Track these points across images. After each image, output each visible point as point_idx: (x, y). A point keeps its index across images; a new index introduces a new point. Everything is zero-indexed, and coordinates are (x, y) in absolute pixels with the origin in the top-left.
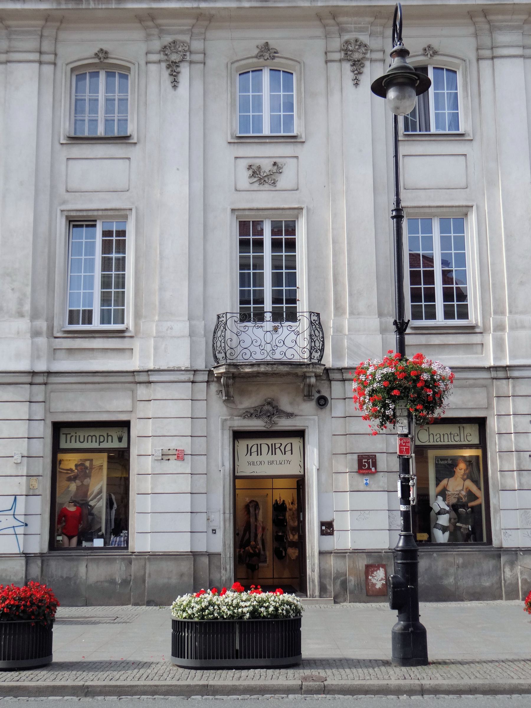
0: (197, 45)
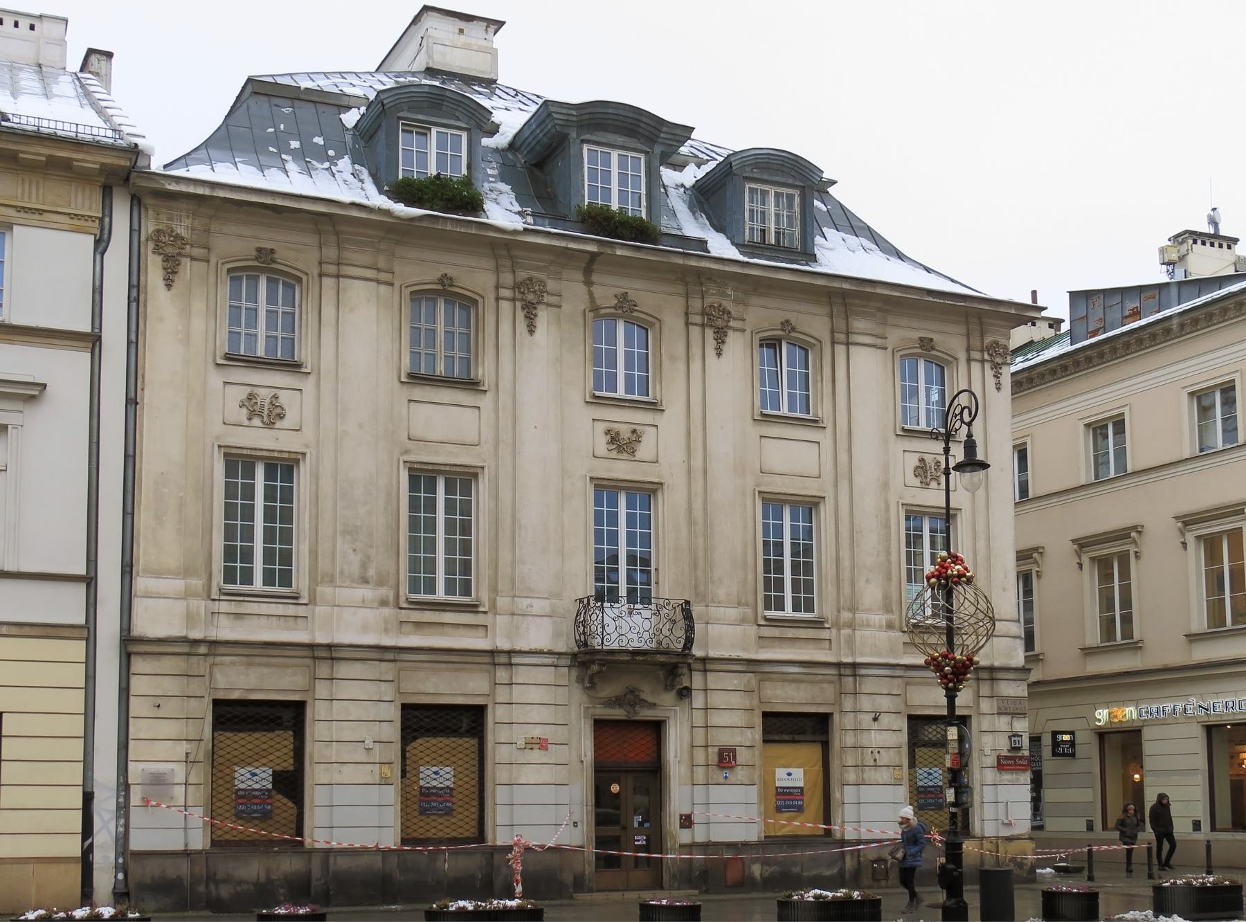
0: (551, 285)
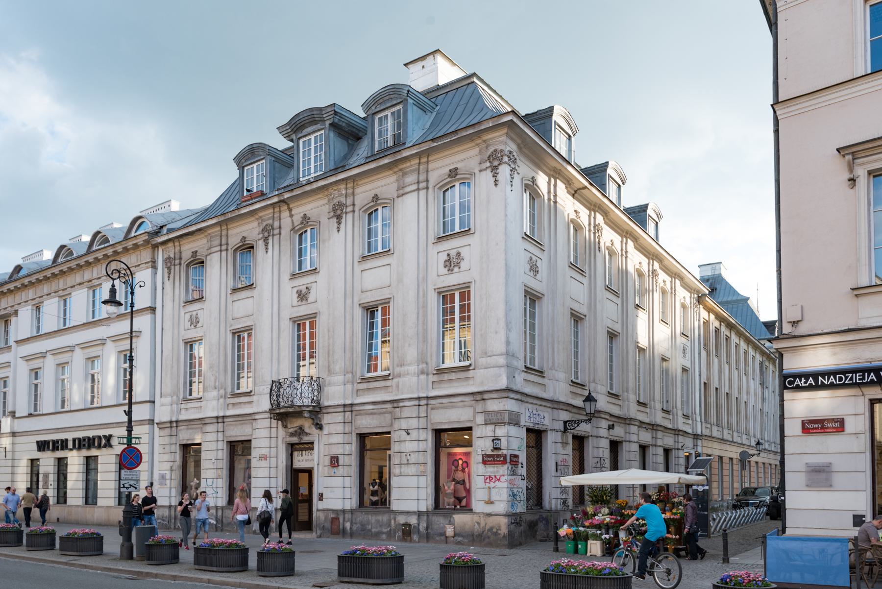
0: (276, 224)
